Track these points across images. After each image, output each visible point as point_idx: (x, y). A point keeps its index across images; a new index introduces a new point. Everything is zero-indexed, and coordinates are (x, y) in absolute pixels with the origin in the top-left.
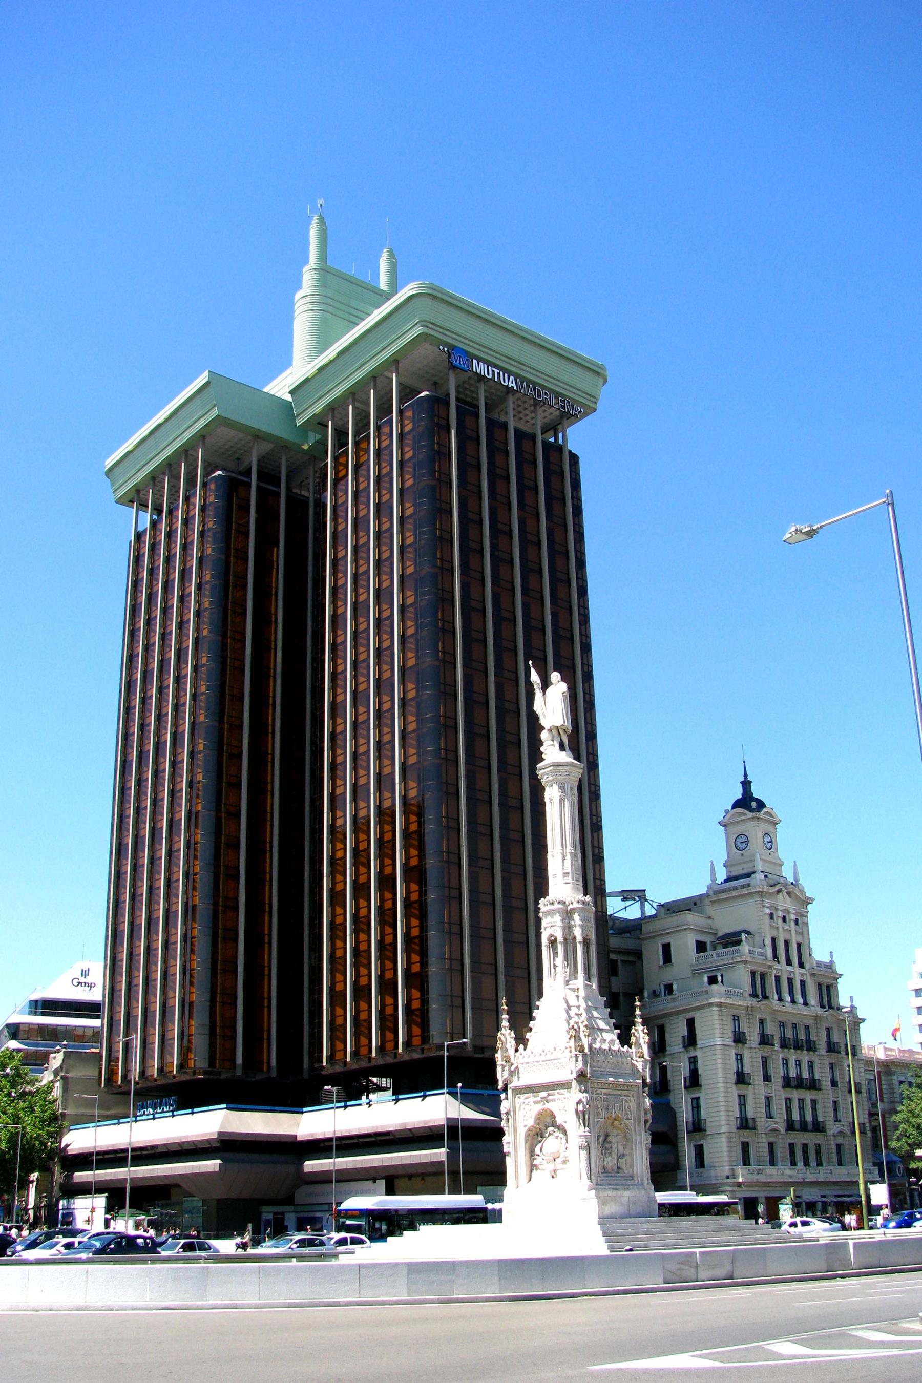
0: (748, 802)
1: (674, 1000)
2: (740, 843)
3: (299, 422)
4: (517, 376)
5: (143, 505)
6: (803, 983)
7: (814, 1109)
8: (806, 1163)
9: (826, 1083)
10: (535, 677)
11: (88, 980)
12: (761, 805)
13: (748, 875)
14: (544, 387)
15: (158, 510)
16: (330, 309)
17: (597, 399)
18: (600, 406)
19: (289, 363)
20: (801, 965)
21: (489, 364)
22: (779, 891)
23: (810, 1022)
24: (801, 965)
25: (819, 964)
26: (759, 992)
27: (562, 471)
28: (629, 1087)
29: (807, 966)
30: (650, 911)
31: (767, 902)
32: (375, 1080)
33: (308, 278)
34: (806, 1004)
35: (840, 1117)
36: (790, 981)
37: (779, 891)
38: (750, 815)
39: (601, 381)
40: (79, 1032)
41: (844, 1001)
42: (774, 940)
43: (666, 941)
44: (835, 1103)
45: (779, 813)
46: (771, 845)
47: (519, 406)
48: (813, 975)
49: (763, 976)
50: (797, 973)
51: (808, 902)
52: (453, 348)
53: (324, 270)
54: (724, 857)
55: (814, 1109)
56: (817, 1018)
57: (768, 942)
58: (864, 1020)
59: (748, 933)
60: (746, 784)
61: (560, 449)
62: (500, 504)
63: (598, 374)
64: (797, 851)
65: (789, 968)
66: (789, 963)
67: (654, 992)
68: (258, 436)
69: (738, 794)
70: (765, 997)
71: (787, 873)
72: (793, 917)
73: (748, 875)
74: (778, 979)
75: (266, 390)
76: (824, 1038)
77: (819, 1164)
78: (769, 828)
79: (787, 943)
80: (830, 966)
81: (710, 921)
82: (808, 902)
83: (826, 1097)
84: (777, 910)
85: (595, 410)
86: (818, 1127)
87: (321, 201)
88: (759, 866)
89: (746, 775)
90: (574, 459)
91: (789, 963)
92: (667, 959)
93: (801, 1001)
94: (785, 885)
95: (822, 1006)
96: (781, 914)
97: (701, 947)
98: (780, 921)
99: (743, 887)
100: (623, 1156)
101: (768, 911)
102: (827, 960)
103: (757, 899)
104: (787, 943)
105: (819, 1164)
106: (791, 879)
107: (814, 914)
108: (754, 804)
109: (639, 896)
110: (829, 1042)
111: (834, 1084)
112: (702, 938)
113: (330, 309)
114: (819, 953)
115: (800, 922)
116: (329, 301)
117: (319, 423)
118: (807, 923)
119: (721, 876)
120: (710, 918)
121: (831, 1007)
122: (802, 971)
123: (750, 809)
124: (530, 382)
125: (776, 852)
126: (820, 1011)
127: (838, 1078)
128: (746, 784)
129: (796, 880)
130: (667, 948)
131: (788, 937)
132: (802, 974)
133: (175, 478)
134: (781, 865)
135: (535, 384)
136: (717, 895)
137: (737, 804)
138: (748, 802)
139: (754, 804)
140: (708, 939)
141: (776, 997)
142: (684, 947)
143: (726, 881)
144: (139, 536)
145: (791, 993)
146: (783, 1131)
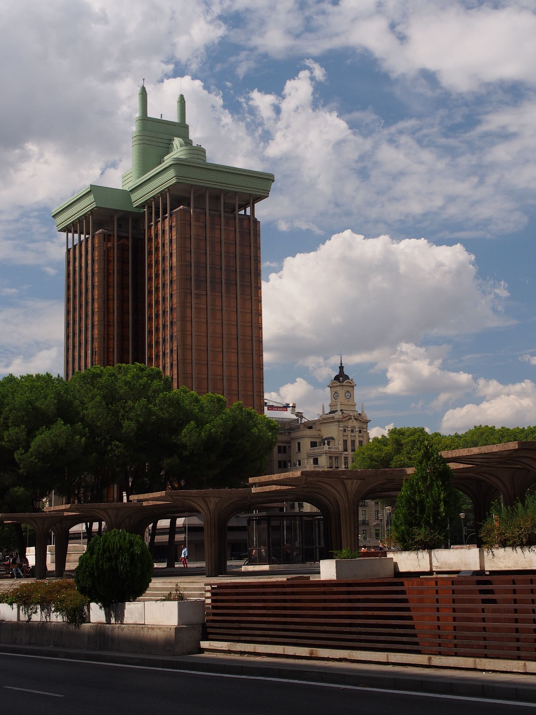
0: (341, 377)
2: (335, 396)
12: (347, 377)
31: (342, 425)
38: (339, 384)
42: (345, 442)
45: (355, 382)
51: (367, 422)
54: (329, 402)
57: (341, 442)
68: (116, 211)
69: (337, 373)
72: (357, 429)
78: (350, 389)
79: (353, 442)
81: (319, 432)
89: (341, 364)
92: (299, 450)
96: (350, 429)
97: (313, 444)
101: (342, 429)
104: (353, 442)
112: (314, 440)
116: (148, 138)
119: (327, 410)
120: (319, 430)
123: (340, 382)
130: (299, 444)
131: (353, 439)
136: (324, 421)
137: (337, 378)
140: (318, 441)
142: (306, 444)
143: (330, 413)
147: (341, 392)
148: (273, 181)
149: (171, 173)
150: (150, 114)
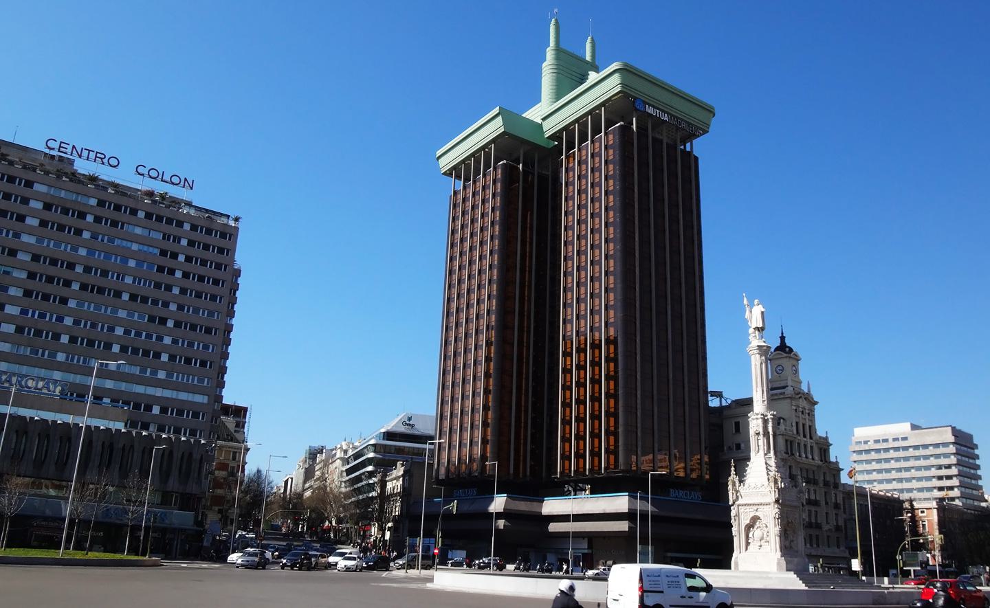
0: (783, 348)
1: (742, 452)
2: (779, 370)
3: (546, 136)
4: (668, 114)
5: (458, 177)
6: (811, 447)
7: (816, 517)
8: (811, 545)
9: (823, 503)
10: (745, 302)
11: (411, 422)
12: (791, 350)
13: (784, 387)
14: (682, 120)
15: (467, 179)
16: (562, 72)
17: (709, 126)
18: (711, 130)
19: (538, 100)
20: (811, 438)
21: (654, 107)
22: (800, 398)
23: (815, 468)
24: (811, 438)
25: (820, 437)
26: (823, 459)
27: (690, 164)
28: (795, 507)
29: (814, 438)
30: (724, 404)
32: (581, 485)
33: (550, 54)
34: (813, 459)
35: (829, 521)
36: (805, 446)
37: (800, 398)
38: (785, 355)
39: (712, 115)
40: (406, 450)
41: (833, 459)
42: (797, 423)
43: (738, 420)
44: (827, 513)
45: (801, 355)
46: (796, 372)
47: (669, 131)
48: (817, 443)
49: (791, 442)
50: (809, 440)
51: (816, 403)
52: (635, 98)
53: (559, 50)
55: (816, 517)
56: (819, 467)
57: (794, 424)
58: (843, 469)
59: (783, 419)
60: (783, 338)
61: (690, 153)
62: (659, 184)
63: (709, 110)
64: (810, 376)
65: (805, 439)
66: (805, 436)
67: (730, 447)
69: (778, 343)
70: (792, 454)
71: (804, 388)
72: (807, 411)
73: (784, 387)
74: (799, 444)
75: (523, 115)
76: (822, 478)
77: (818, 546)
78: (794, 362)
80: (826, 439)
82: (816, 403)
83: (823, 510)
84: (799, 407)
85: (708, 132)
86: (818, 526)
87: (556, 10)
88: (790, 383)
89: (782, 333)
90: (696, 159)
91: (805, 436)
93: (804, 456)
94: (804, 394)
95: (821, 461)
96: (801, 409)
98: (800, 413)
99: (781, 394)
100: (793, 541)
101: (794, 408)
102: (825, 436)
103: (789, 400)
104: (804, 425)
105: (818, 546)
106: (806, 391)
107: (818, 411)
108: (787, 349)
109: (719, 395)
110: (824, 480)
111: (827, 503)
113: (562, 72)
114: (820, 432)
115: (811, 414)
116: (561, 68)
117: (556, 136)
118: (814, 415)
121: (826, 462)
122: (811, 441)
124: (675, 117)
125: (798, 376)
126: (820, 463)
127: (828, 500)
128: (783, 338)
129: (809, 391)
130: (737, 424)
131: (804, 422)
132: (811, 443)
133: (477, 162)
134: (801, 383)
135: (678, 118)
138: (783, 348)
139: (787, 349)
141: (798, 454)
144: (455, 193)
145: (806, 453)
146: (834, 530)
147: (786, 363)
148: (714, 115)
149: (616, 79)
150: (562, 46)
